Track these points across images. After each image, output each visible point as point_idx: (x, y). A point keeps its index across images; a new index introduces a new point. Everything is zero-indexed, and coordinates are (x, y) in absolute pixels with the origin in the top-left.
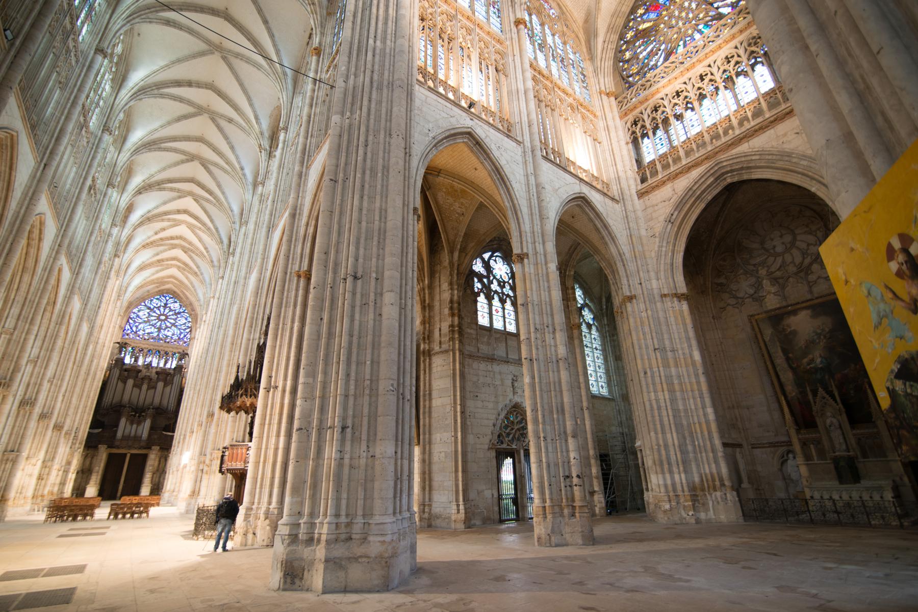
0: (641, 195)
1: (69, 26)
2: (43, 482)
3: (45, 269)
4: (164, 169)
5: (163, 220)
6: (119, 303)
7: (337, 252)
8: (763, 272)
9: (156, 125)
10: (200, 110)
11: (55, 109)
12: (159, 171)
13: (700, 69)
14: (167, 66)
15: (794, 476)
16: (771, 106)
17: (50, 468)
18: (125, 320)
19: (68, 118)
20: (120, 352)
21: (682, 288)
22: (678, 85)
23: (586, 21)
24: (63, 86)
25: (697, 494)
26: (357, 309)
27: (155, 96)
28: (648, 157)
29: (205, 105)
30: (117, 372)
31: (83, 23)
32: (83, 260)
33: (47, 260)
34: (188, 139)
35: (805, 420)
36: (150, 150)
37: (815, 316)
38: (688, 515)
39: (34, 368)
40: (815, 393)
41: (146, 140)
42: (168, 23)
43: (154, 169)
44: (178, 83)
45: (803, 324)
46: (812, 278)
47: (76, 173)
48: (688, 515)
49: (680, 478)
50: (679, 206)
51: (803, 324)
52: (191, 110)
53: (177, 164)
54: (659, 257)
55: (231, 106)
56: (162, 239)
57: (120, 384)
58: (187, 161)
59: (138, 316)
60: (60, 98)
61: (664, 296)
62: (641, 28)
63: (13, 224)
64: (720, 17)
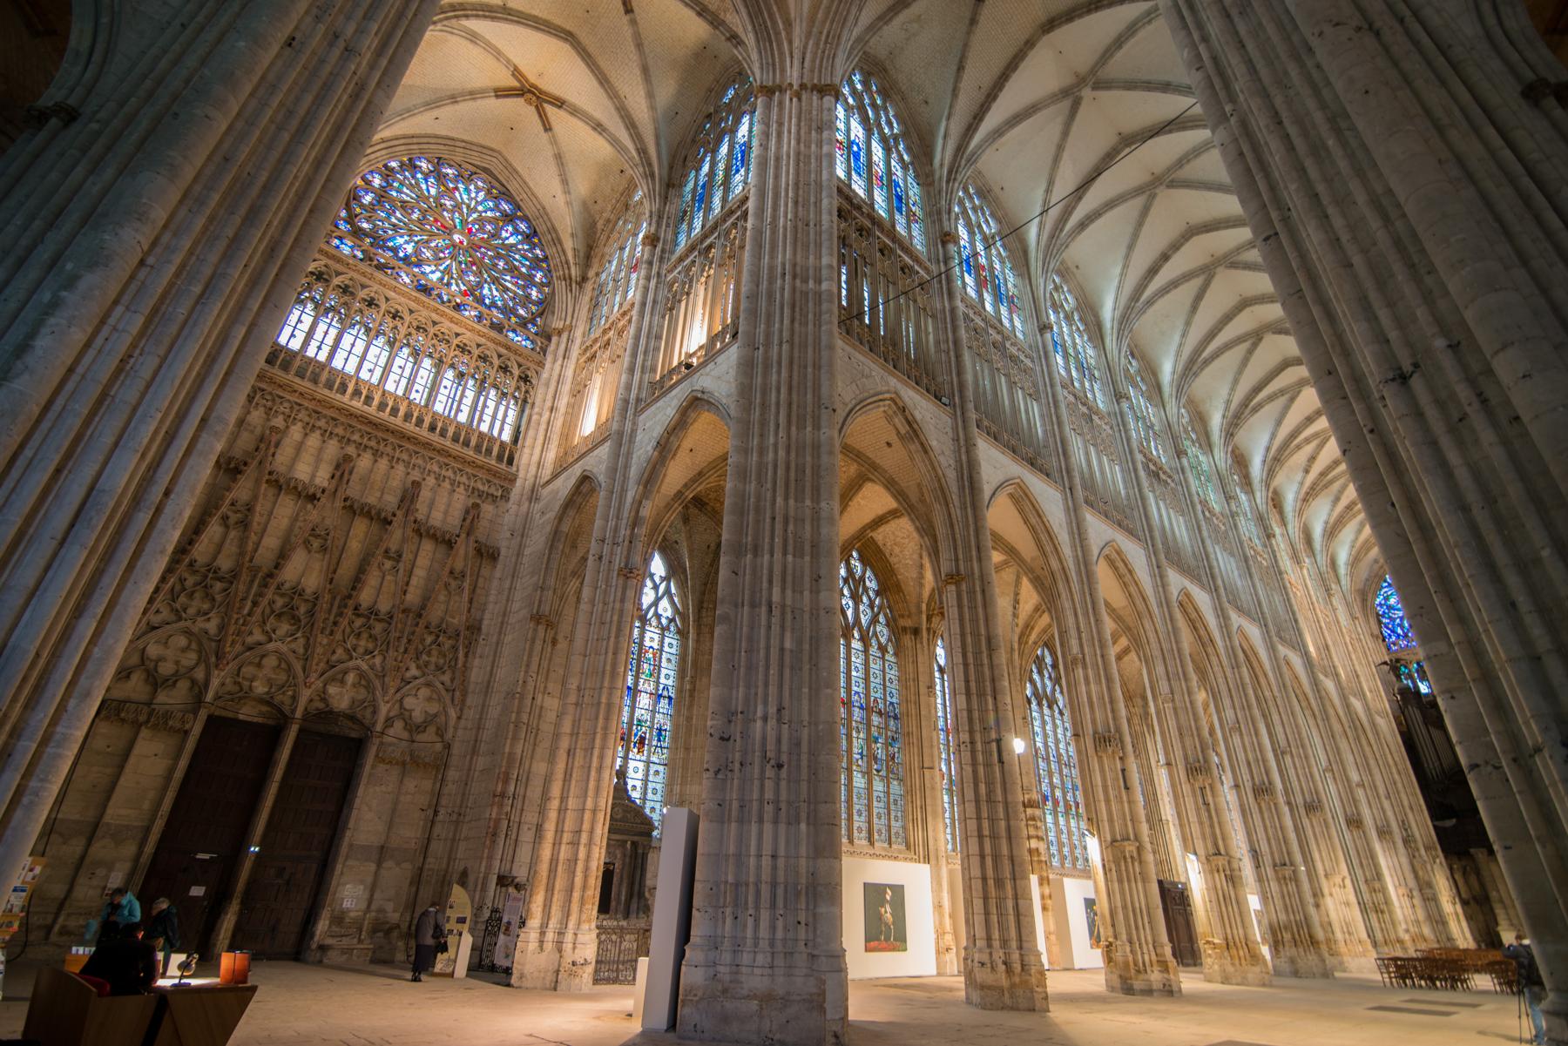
1: (999, 338)
2: (1387, 916)
3: (1160, 605)
4: (1236, 381)
5: (1299, 447)
6: (1337, 601)
9: (1177, 338)
10: (1207, 272)
11: (1044, 424)
12: (1233, 389)
14: (1125, 266)
17: (1384, 890)
18: (1373, 621)
19: (1060, 424)
20: (1398, 677)
24: (1035, 396)
26: (1446, 442)
27: (1143, 311)
29: (1208, 260)
30: (1415, 714)
31: (1011, 320)
32: (1211, 568)
33: (1156, 592)
34: (1227, 319)
36: (1196, 375)
39: (1241, 735)
41: (1180, 368)
42: (1082, 225)
43: (1224, 392)
44: (1153, 271)
47: (1122, 471)
52: (1196, 283)
53: (1245, 362)
55: (1234, 226)
56: (1323, 474)
57: (1435, 733)
58: (1255, 346)
59: (1390, 607)
60: (1041, 410)
63: (1079, 572)
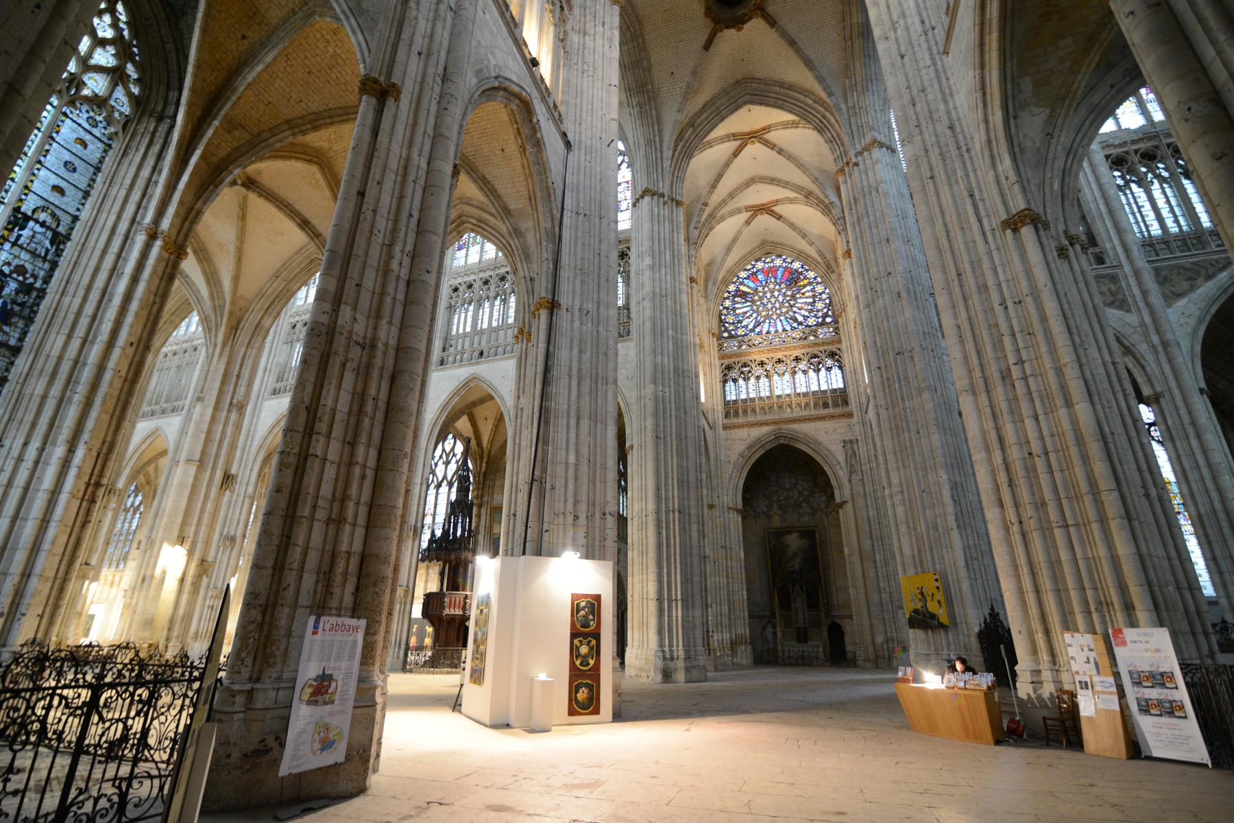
0: (725, 427)
7: (666, 491)
8: (775, 498)
13: (780, 355)
15: (770, 637)
16: (816, 406)
21: (740, 506)
22: (763, 357)
23: (710, 264)
25: (734, 645)
28: (731, 397)
35: (786, 604)
37: (800, 538)
38: (728, 660)
40: (794, 586)
45: (794, 541)
46: (801, 511)
48: (728, 660)
49: (727, 636)
50: (750, 447)
51: (794, 541)
54: (730, 478)
61: (729, 508)
62: (742, 288)
64: (795, 320)
